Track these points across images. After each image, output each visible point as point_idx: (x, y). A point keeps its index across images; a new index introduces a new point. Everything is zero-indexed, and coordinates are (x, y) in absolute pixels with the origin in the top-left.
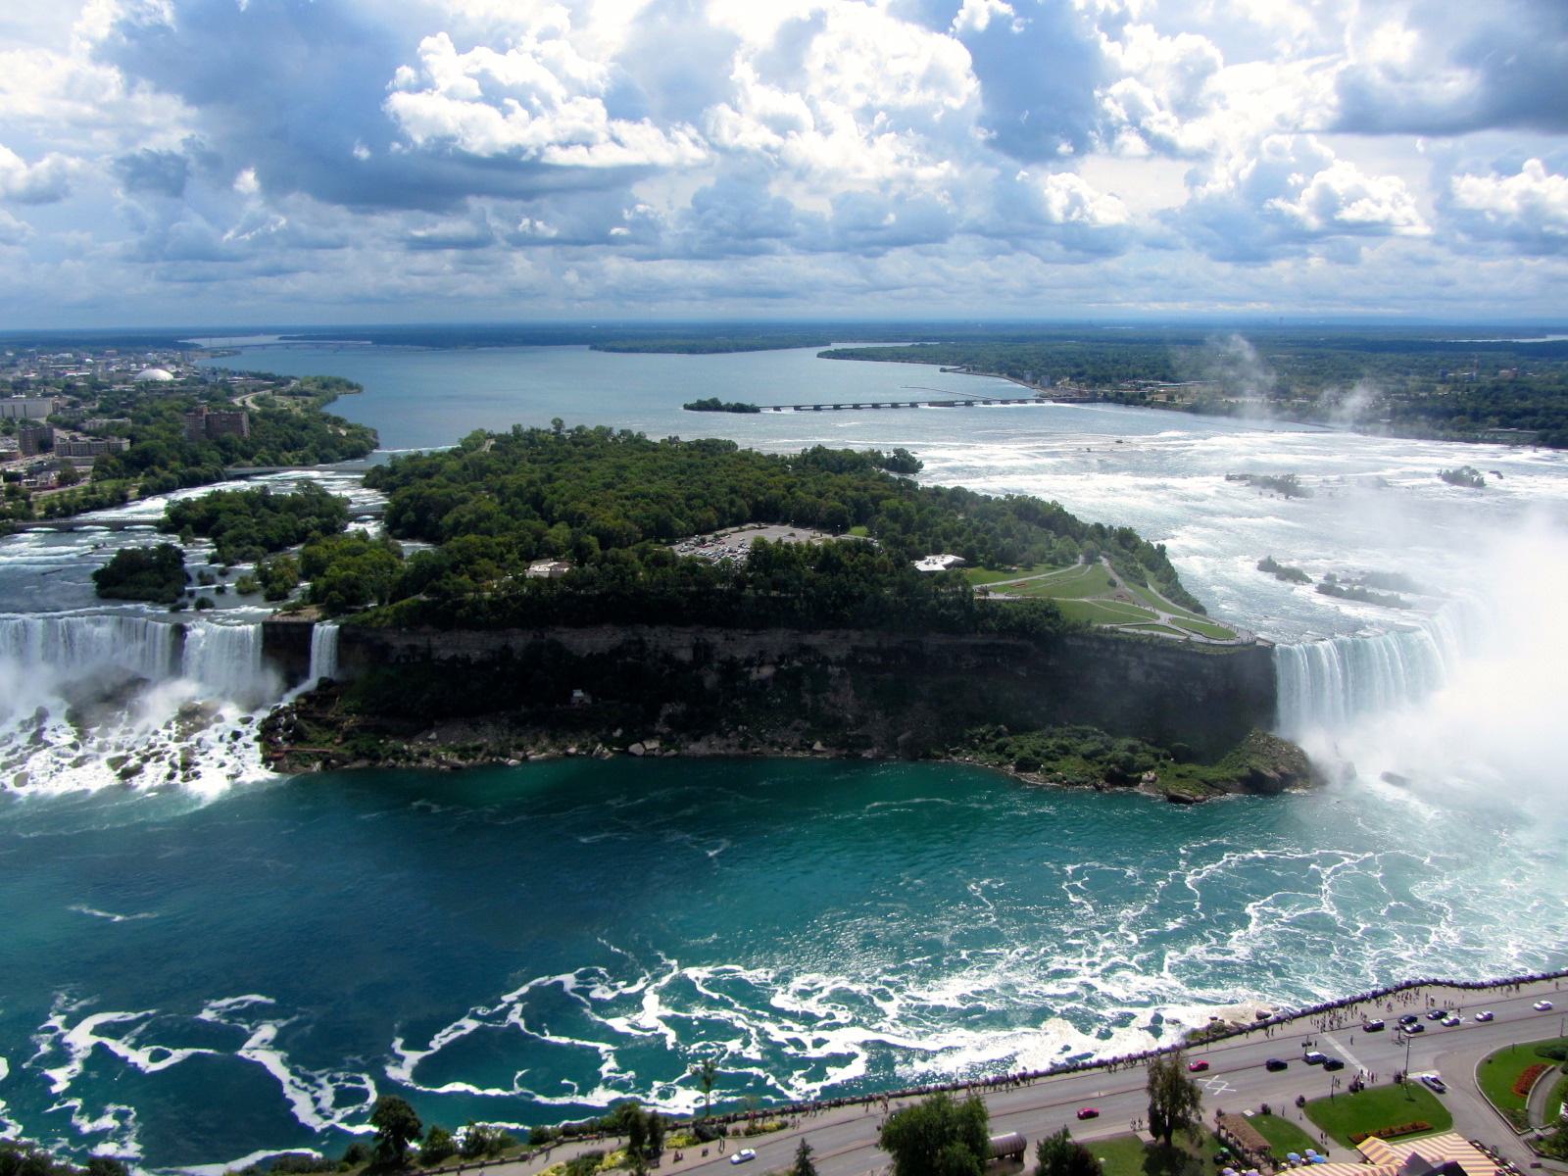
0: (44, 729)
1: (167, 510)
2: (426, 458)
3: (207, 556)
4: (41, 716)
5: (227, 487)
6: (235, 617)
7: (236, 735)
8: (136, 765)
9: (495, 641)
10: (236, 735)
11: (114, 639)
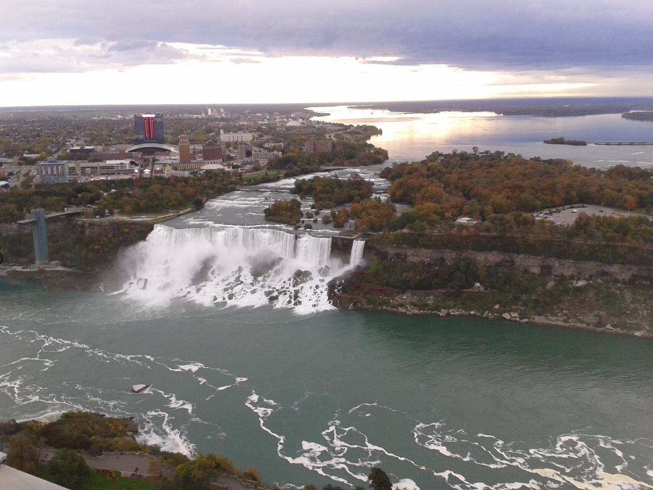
0: (241, 276)
1: (295, 183)
2: (411, 165)
3: (310, 206)
4: (240, 269)
5: (320, 175)
6: (320, 234)
7: (317, 287)
10: (317, 287)
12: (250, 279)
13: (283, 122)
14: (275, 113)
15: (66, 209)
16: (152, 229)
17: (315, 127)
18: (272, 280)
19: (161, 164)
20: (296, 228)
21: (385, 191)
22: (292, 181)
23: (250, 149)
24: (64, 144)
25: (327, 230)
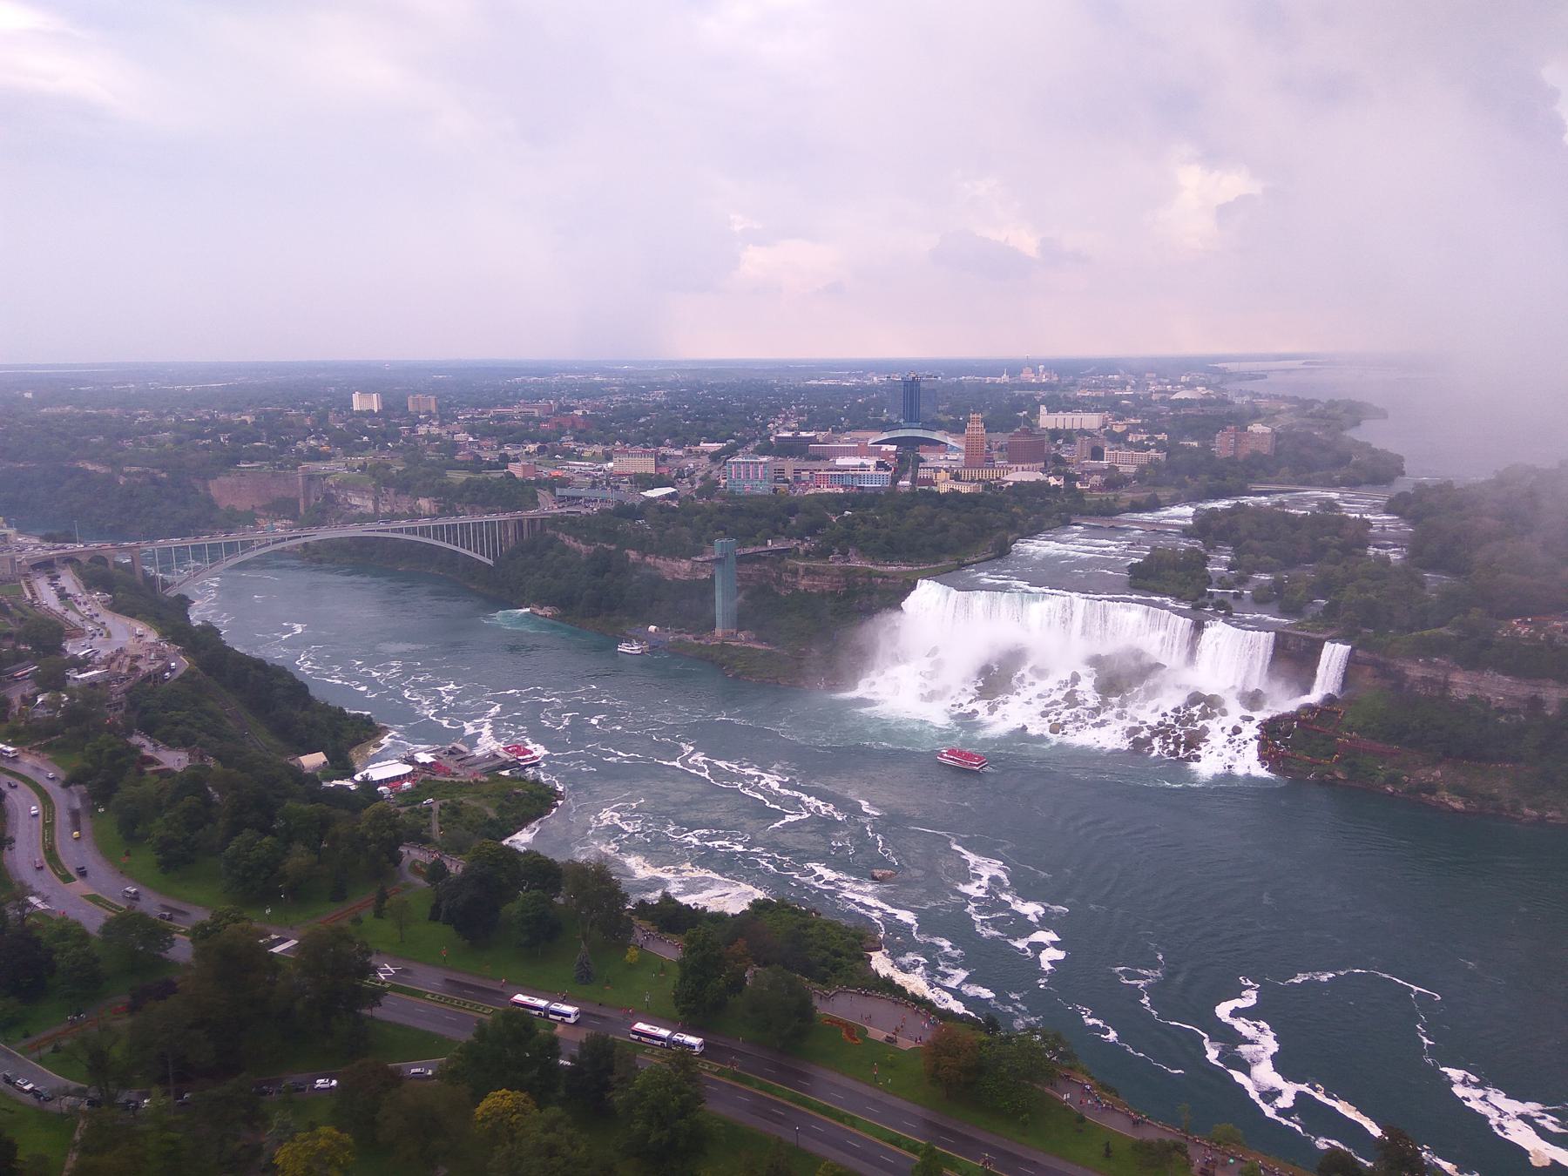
1: (1194, 517)
3: (1226, 563)
4: (1075, 679)
5: (1249, 501)
6: (1249, 622)
7: (1237, 730)
8: (1146, 737)
9: (1524, 690)
10: (1237, 730)
11: (1140, 626)
12: (1093, 700)
13: (1166, 392)
14: (1147, 375)
15: (770, 542)
16: (913, 587)
17: (1231, 403)
18: (1138, 708)
19: (931, 468)
20: (1195, 608)
21: (1398, 542)
22: (1188, 511)
23: (1099, 444)
24: (764, 427)
25: (1265, 616)
